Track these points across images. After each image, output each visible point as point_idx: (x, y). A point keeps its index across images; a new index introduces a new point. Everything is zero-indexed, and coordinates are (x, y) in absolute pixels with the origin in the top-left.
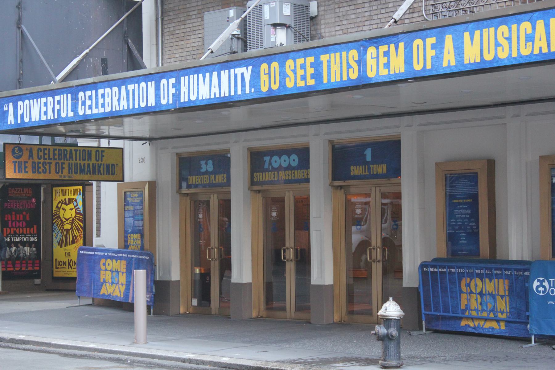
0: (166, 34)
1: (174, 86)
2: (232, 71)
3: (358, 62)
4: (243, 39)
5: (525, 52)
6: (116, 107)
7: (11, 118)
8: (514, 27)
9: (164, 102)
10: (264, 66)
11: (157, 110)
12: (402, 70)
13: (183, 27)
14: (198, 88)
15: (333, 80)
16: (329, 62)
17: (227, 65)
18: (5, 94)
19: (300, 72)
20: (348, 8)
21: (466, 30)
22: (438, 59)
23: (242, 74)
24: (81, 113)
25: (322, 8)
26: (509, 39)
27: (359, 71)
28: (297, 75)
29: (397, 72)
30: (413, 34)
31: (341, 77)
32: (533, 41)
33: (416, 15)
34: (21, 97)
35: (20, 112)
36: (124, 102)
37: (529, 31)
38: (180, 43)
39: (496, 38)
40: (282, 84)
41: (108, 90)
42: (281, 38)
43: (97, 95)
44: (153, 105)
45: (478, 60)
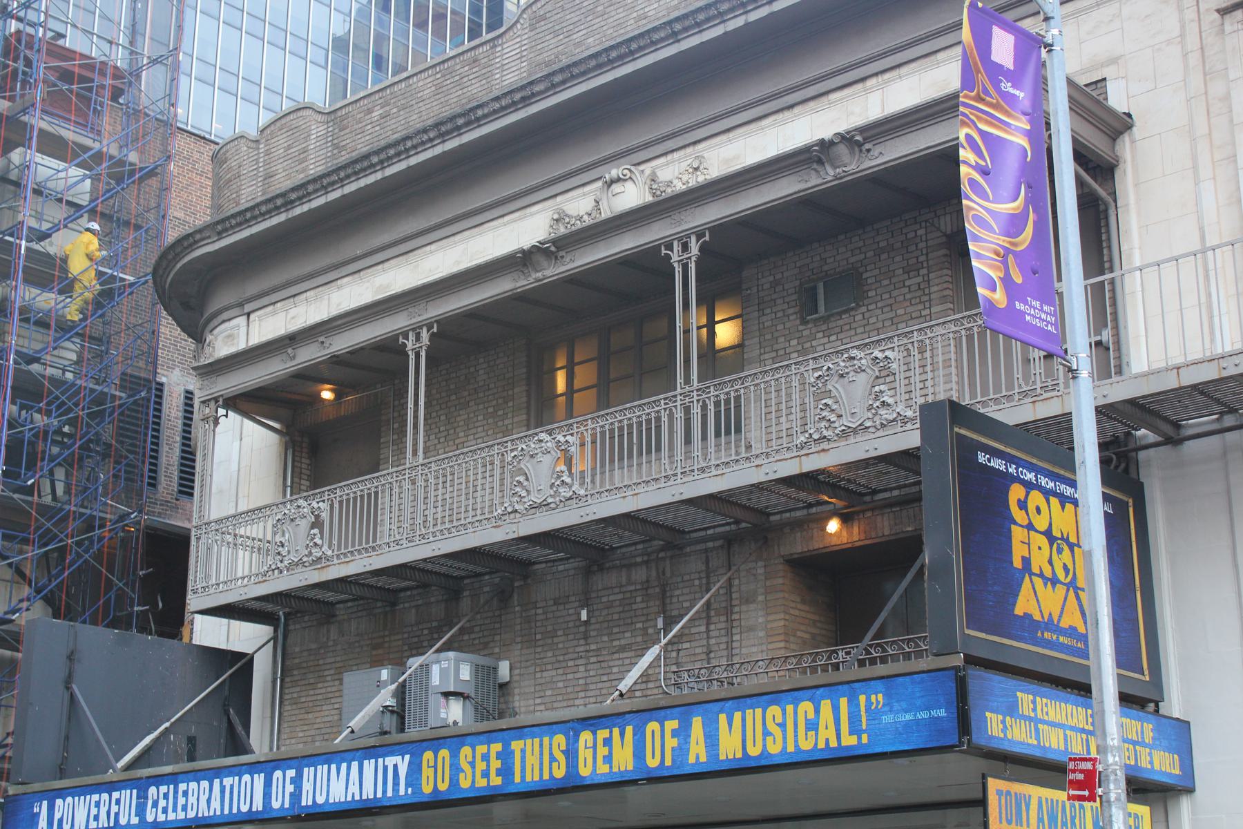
0: (286, 703)
1: (293, 781)
2: (380, 760)
3: (566, 753)
4: (399, 713)
5: (806, 745)
6: (203, 811)
8: (790, 708)
9: (276, 805)
10: (428, 755)
11: (266, 816)
12: (630, 767)
13: (312, 692)
14: (328, 786)
15: (528, 779)
16: (523, 751)
17: (372, 751)
18: (37, 787)
19: (481, 766)
20: (554, 673)
21: (721, 712)
22: (681, 751)
23: (395, 766)
24: (150, 818)
25: (517, 672)
26: (782, 725)
27: (567, 767)
28: (476, 770)
29: (622, 769)
30: (647, 715)
32: (817, 730)
33: (651, 685)
34: (62, 793)
35: (57, 816)
36: (216, 804)
37: (811, 715)
38: (306, 716)
39: (764, 724)
40: (454, 782)
41: (193, 785)
42: (455, 712)
43: (176, 792)
44: (260, 809)
45: (739, 755)
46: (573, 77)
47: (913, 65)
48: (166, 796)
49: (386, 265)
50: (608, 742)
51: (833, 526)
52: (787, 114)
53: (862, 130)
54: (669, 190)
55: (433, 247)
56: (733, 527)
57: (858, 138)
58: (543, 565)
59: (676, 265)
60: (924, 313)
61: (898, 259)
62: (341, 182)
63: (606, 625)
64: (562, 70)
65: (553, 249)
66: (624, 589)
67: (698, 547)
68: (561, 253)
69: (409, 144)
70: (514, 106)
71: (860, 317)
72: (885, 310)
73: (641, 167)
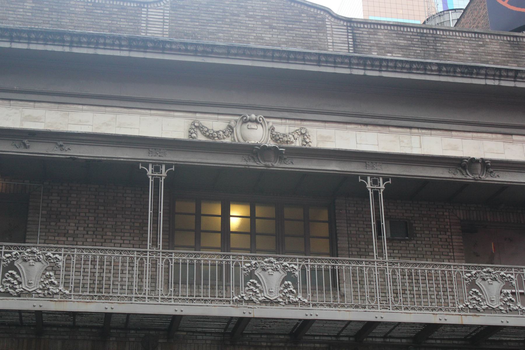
46: (244, 54)
47: (439, 132)
49: (37, 104)
52: (364, 127)
53: (493, 161)
54: (285, 139)
55: (85, 107)
56: (334, 339)
57: (489, 164)
58: (185, 333)
59: (370, 190)
60: (450, 254)
61: (434, 223)
62: (29, 40)
64: (239, 48)
65: (284, 152)
67: (308, 345)
68: (285, 157)
69: (102, 41)
70: (195, 53)
71: (412, 245)
72: (427, 246)
73: (268, 120)
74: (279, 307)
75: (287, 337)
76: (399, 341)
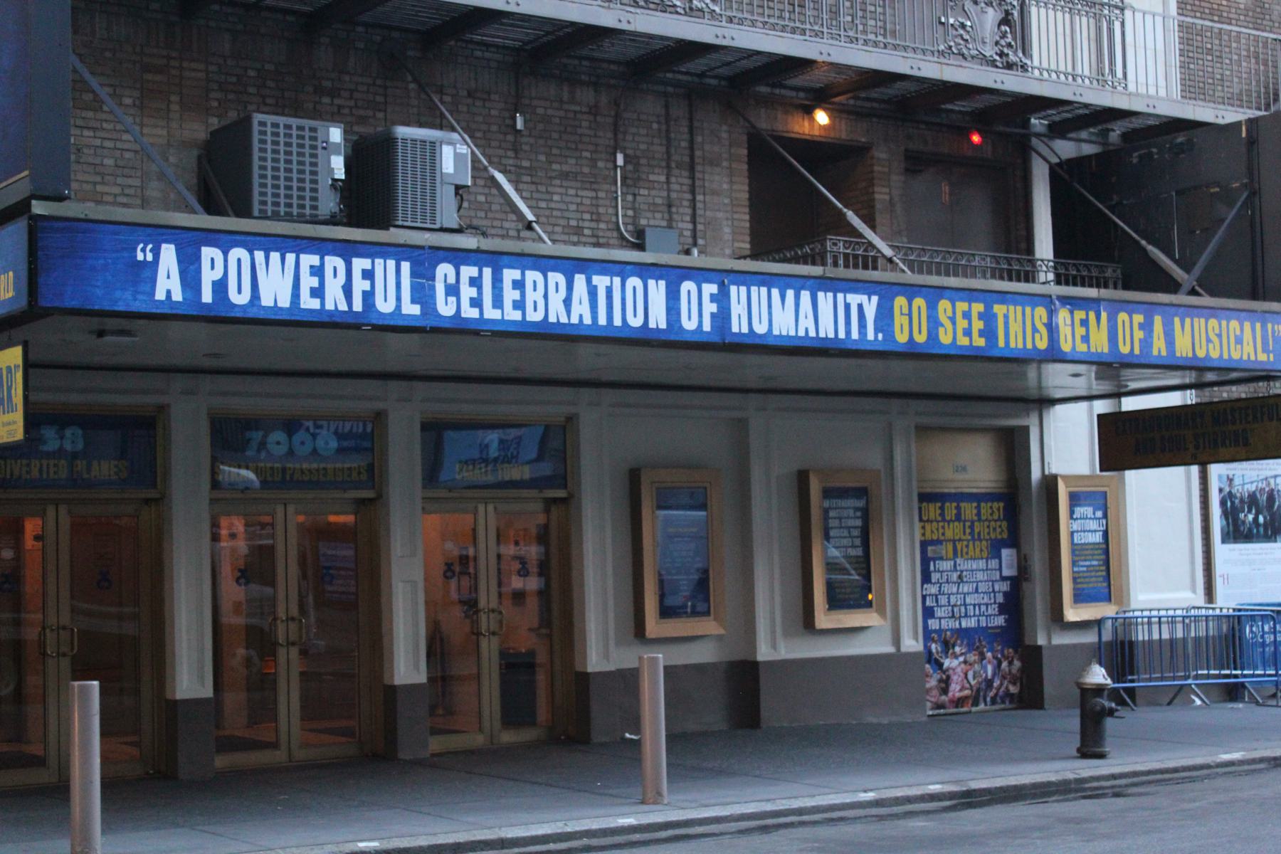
6: (557, 313)
7: (168, 283)
8: (1224, 323)
11: (673, 337)
14: (770, 314)
15: (1012, 345)
16: (1006, 317)
19: (962, 324)
23: (860, 307)
26: (1219, 336)
31: (1025, 343)
32: (1241, 343)
33: (602, 226)
35: (209, 277)
37: (1238, 332)
40: (933, 336)
41: (532, 276)
43: (497, 281)
44: (663, 325)
45: (1190, 355)
48: (475, 282)
50: (1084, 323)
51: (822, 117)
56: (696, 80)
63: (541, 142)
66: (566, 107)
74: (675, 16)
75: (621, 69)
76: (794, 94)
